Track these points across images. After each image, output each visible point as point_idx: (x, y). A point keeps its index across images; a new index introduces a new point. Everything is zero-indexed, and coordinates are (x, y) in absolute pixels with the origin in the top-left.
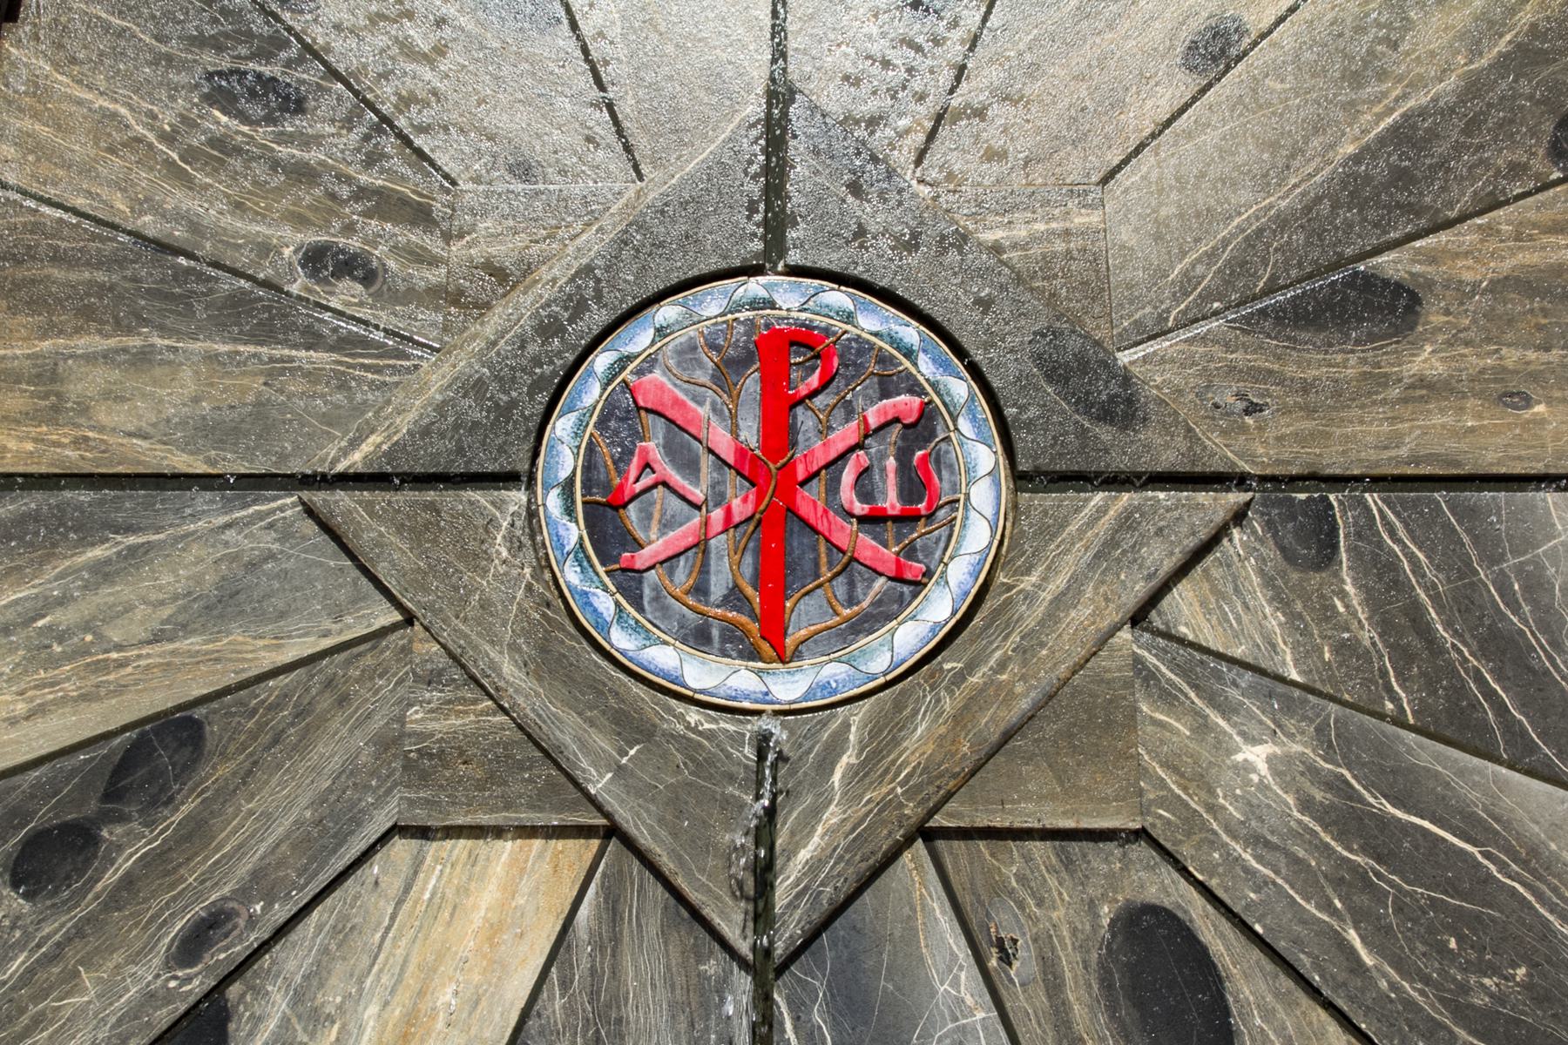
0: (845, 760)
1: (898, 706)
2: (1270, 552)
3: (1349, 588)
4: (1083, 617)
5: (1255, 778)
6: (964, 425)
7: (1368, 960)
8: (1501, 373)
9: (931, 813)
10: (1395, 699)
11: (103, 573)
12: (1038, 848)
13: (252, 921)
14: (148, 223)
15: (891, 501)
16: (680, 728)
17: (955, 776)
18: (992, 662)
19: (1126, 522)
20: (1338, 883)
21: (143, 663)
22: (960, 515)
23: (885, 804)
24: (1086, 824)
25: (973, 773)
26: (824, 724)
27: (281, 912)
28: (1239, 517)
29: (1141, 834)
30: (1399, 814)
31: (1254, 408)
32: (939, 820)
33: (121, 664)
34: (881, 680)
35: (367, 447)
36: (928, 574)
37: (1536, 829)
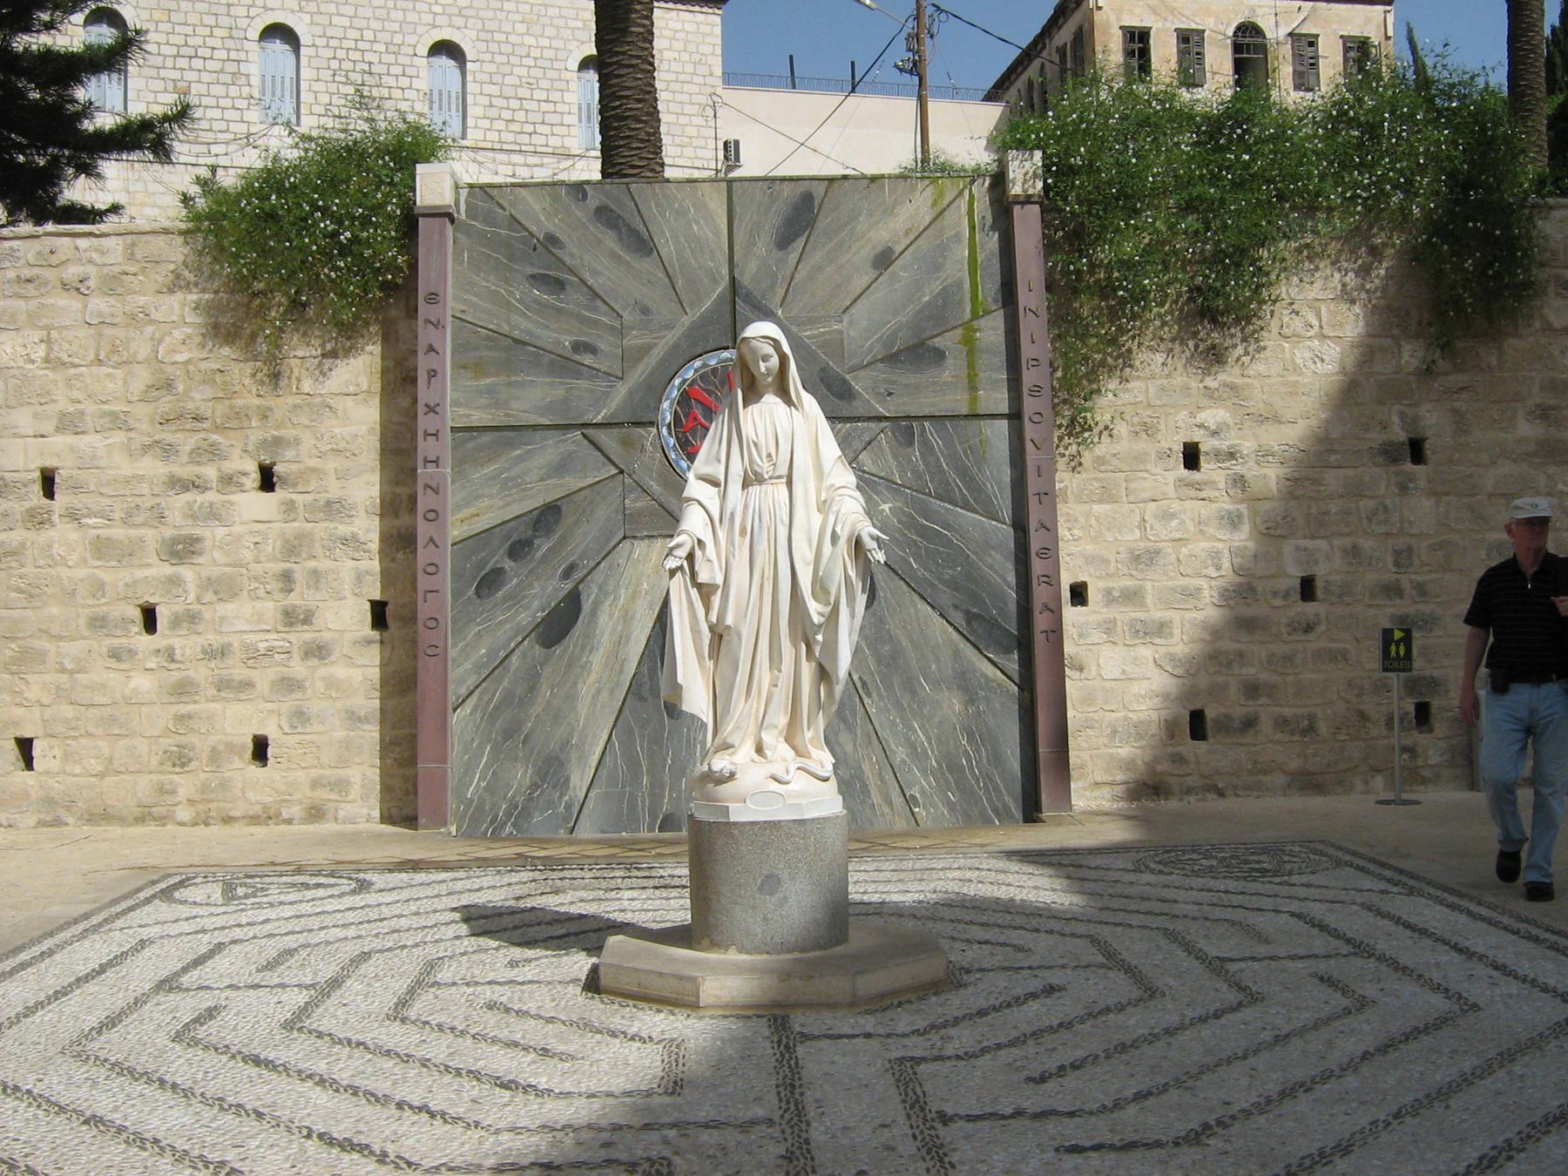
11: (520, 459)
13: (584, 566)
14: (516, 334)
27: (592, 564)
31: (890, 394)
33: (531, 489)
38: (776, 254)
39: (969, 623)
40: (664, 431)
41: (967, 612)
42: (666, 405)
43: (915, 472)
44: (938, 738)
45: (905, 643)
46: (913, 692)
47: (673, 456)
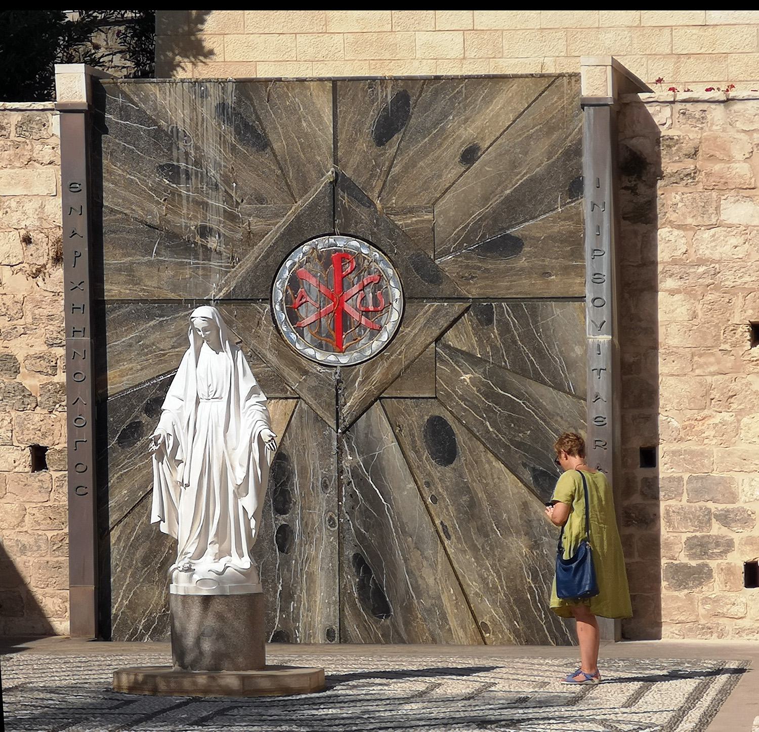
0: (359, 379)
1: (373, 364)
2: (475, 321)
3: (496, 331)
4: (422, 340)
5: (466, 383)
6: (392, 283)
7: (491, 430)
8: (544, 267)
9: (381, 394)
10: (505, 362)
12: (408, 401)
15: (371, 308)
16: (315, 371)
17: (387, 384)
18: (398, 353)
19: (437, 311)
20: (485, 411)
21: (171, 354)
22: (390, 310)
23: (369, 391)
24: (421, 396)
25: (392, 383)
26: (353, 370)
28: (467, 310)
29: (436, 398)
30: (502, 392)
32: (383, 395)
34: (369, 358)
35: (223, 292)
36: (381, 327)
37: (537, 396)
38: (376, 150)
39: (535, 478)
40: (278, 307)
41: (534, 470)
42: (278, 284)
43: (494, 348)
44: (507, 578)
45: (481, 495)
46: (486, 535)
47: (284, 328)
